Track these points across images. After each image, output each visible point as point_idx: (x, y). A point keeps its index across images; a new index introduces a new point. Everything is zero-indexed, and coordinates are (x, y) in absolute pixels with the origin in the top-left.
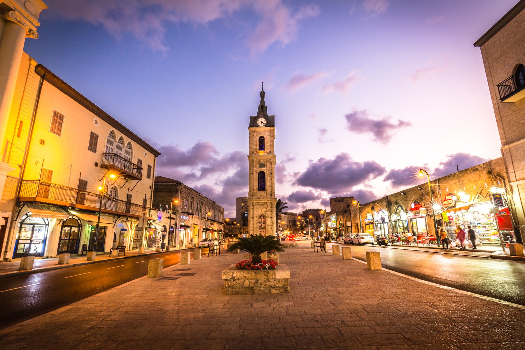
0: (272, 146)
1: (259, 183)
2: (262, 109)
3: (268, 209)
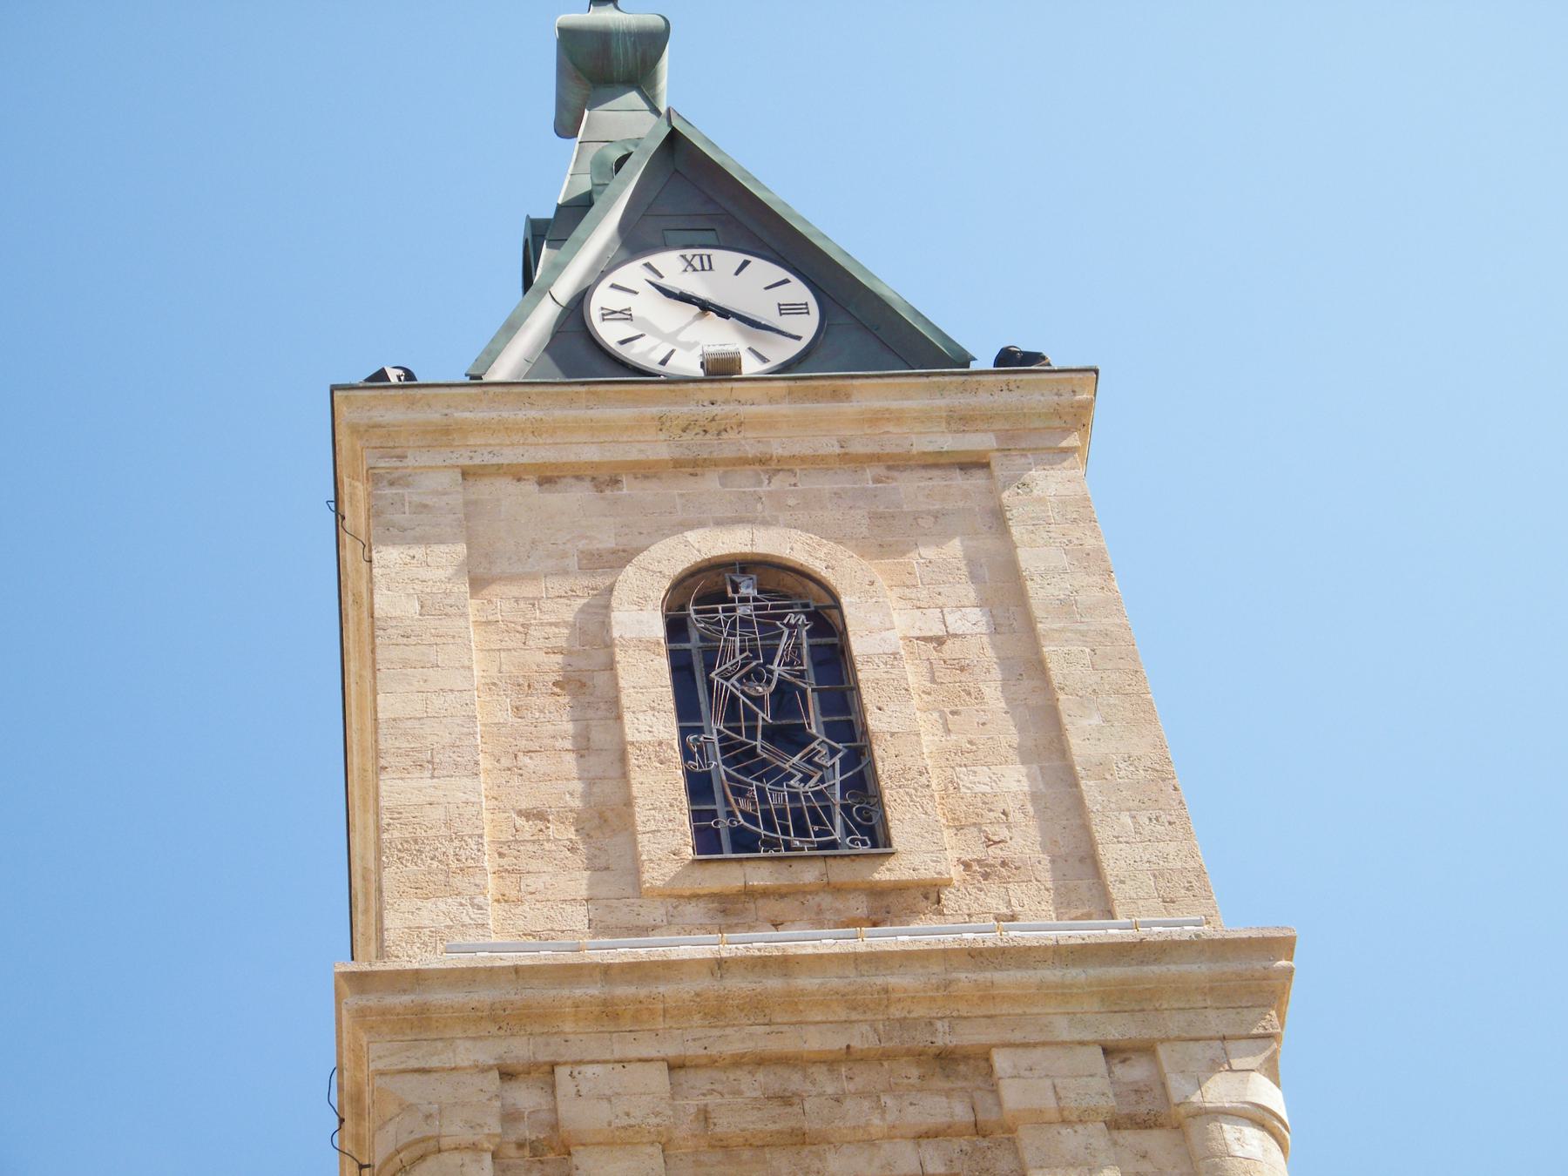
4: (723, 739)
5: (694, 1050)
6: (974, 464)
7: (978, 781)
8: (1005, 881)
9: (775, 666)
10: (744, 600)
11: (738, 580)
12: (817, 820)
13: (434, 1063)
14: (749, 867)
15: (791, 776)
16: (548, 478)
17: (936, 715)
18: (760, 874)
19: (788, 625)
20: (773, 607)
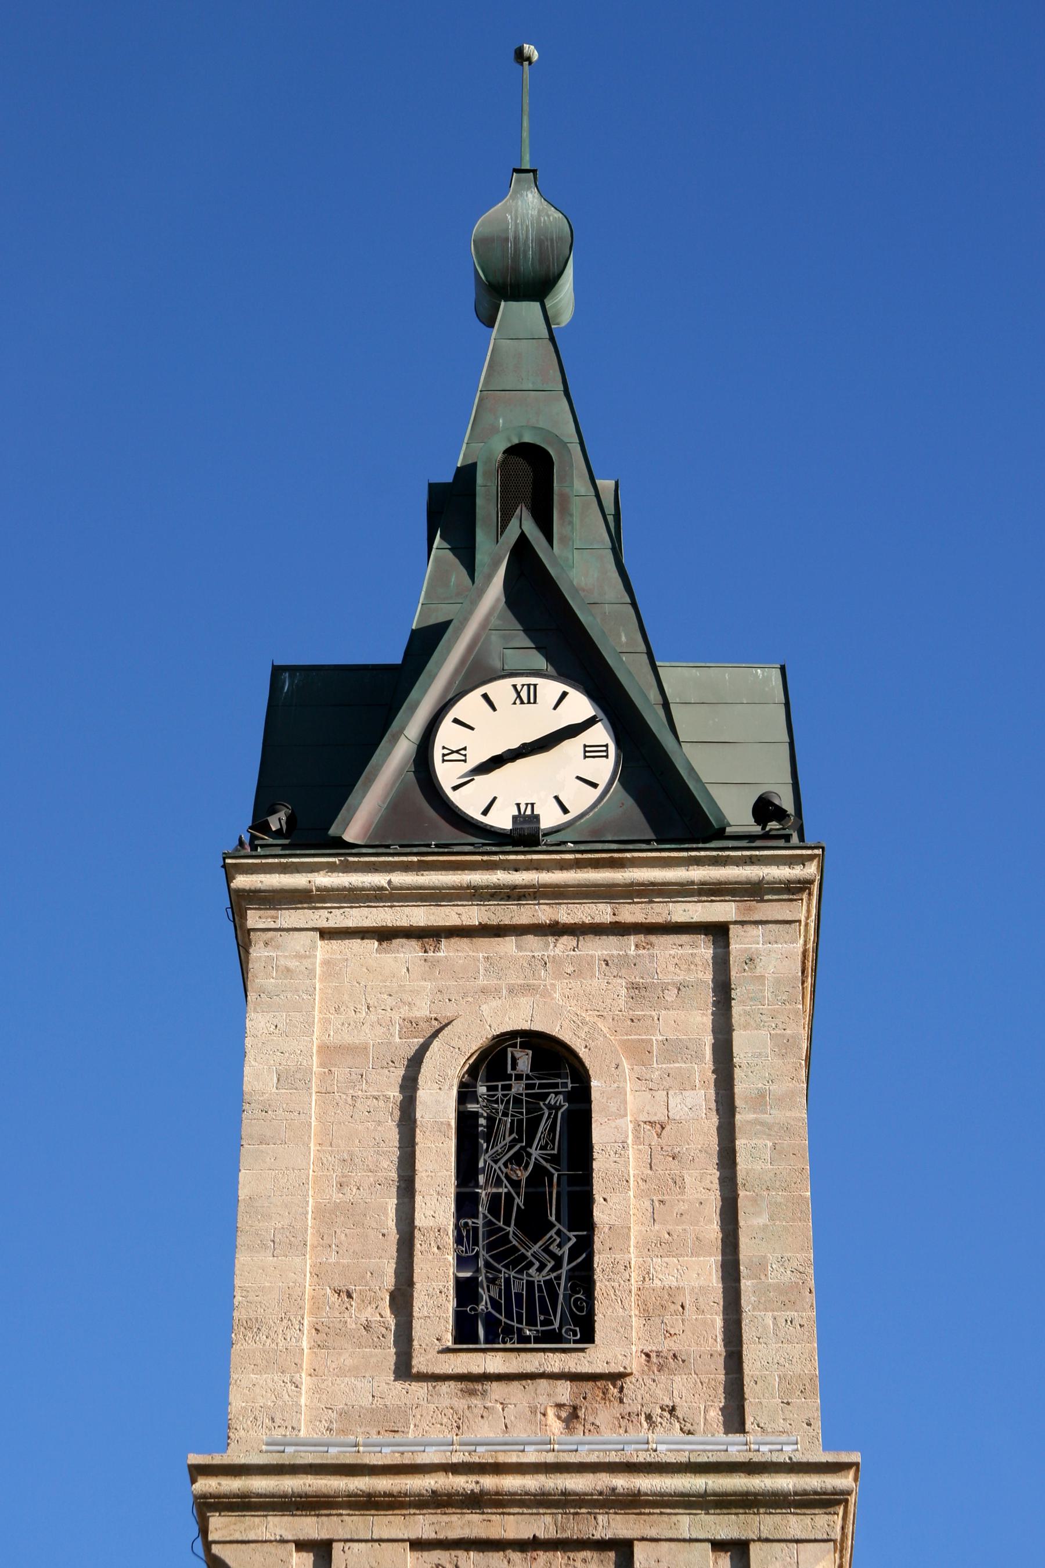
4: (489, 1223)
5: (428, 1534)
6: (719, 932)
7: (667, 1273)
8: (672, 1372)
9: (532, 1151)
10: (519, 1077)
11: (517, 1055)
12: (544, 1311)
13: (252, 1537)
14: (489, 1356)
15: (531, 1264)
16: (384, 935)
17: (648, 1203)
18: (494, 1363)
19: (550, 1107)
20: (541, 1086)
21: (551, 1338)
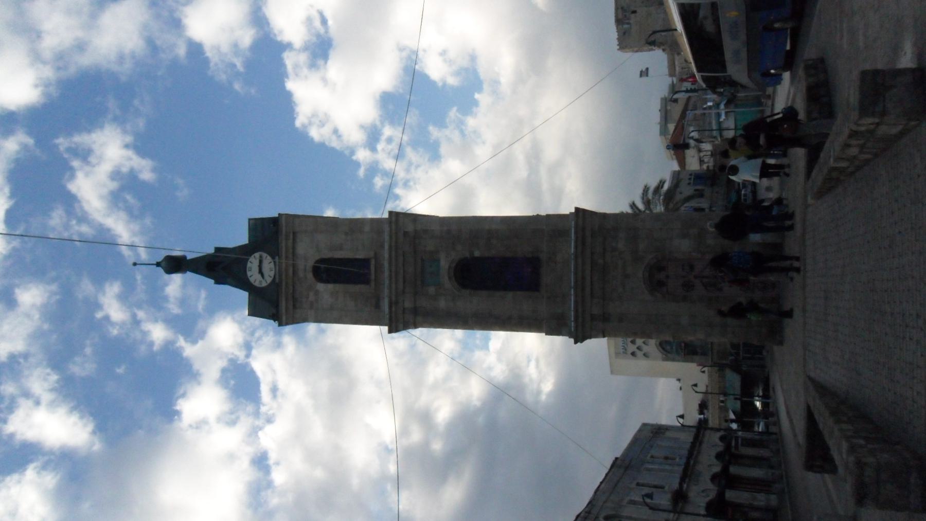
0: (355, 225)
1: (507, 288)
2: (221, 267)
3: (621, 245)
18: (373, 277)
21: (368, 267)
